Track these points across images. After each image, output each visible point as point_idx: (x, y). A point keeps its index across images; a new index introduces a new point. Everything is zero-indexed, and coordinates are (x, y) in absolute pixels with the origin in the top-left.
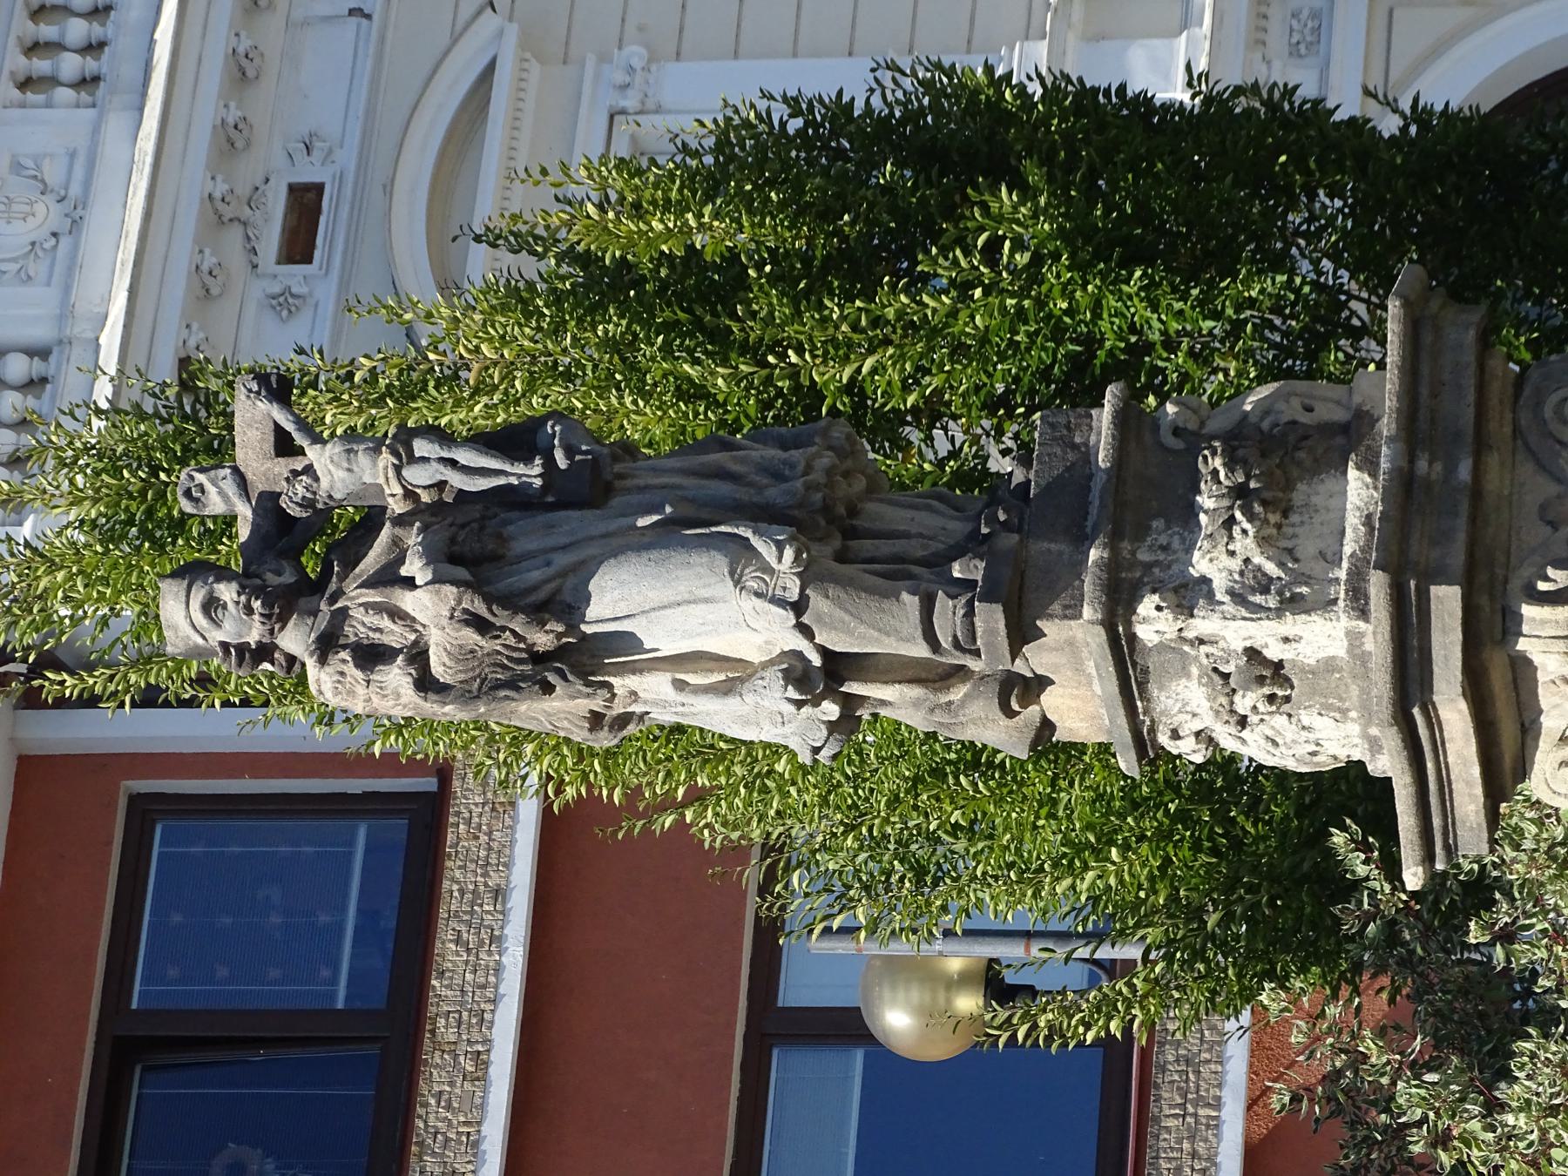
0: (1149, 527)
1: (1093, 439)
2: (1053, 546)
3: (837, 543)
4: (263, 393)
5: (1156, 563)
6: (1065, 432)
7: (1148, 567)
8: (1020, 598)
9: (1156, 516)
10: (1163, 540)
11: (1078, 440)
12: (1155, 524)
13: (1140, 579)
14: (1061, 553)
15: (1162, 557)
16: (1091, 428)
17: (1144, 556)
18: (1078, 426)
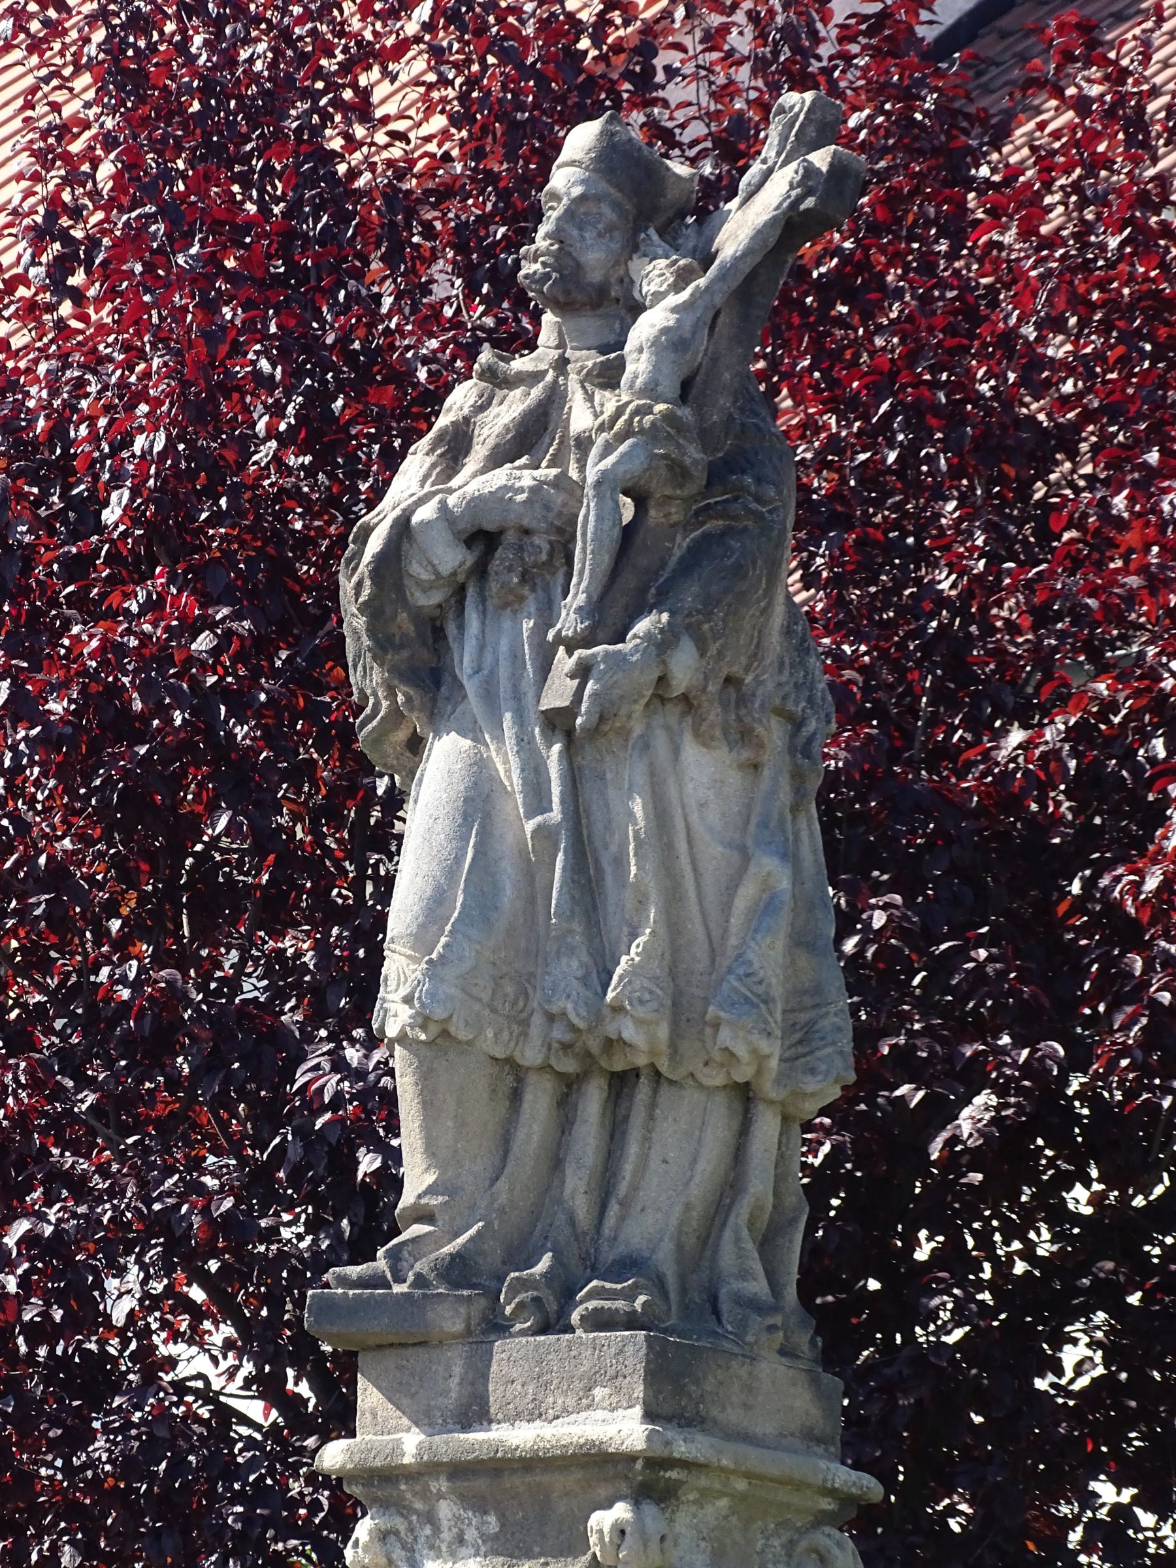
0: (486, 1513)
1: (600, 1414)
2: (454, 1383)
3: (569, 1066)
4: (794, 193)
5: (437, 1530)
6: (611, 1372)
7: (430, 1518)
8: (391, 1345)
9: (502, 1518)
10: (471, 1534)
11: (599, 1392)
12: (492, 1519)
13: (411, 1510)
14: (446, 1392)
15: (446, 1536)
16: (612, 1410)
17: (446, 1510)
18: (618, 1390)
